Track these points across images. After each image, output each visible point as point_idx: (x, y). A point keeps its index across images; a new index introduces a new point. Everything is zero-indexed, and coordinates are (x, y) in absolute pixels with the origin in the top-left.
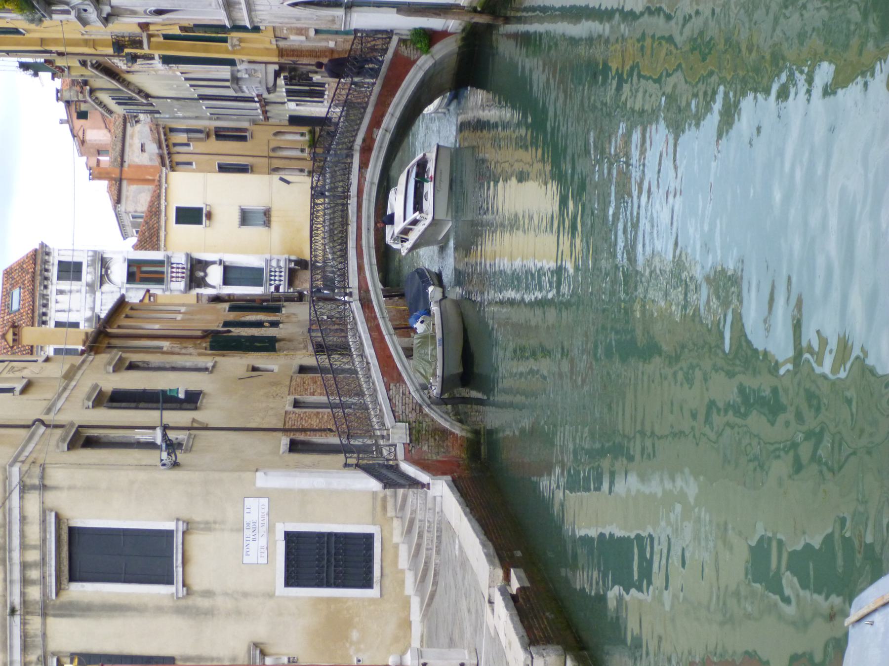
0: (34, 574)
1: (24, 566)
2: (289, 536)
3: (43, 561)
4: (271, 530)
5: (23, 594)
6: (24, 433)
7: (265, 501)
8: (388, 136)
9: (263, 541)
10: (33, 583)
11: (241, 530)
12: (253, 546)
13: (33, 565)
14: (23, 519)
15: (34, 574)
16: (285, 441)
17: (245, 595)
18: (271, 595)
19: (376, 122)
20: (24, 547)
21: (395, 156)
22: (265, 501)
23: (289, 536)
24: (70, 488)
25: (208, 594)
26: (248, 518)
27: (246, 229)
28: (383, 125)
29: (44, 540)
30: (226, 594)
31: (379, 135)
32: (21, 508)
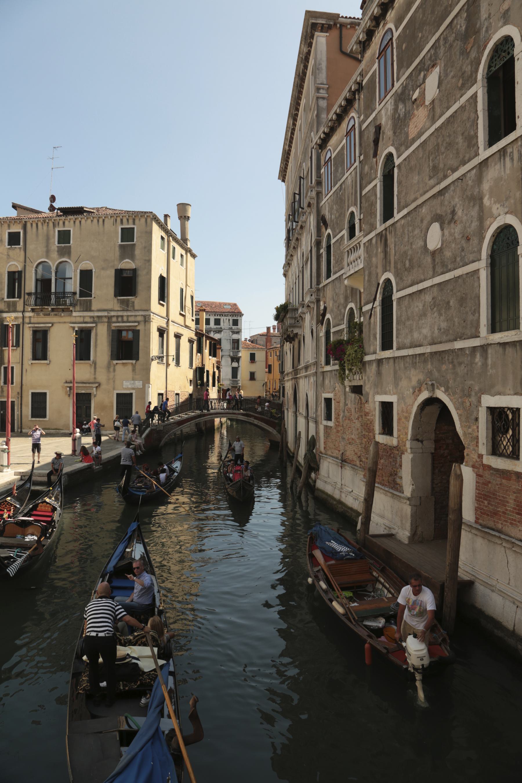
0: (120, 319)
1: (122, 316)
2: (131, 394)
3: (123, 322)
4: (133, 389)
5: (114, 316)
6: (164, 315)
7: (141, 387)
8: (252, 422)
9: (130, 386)
10: (117, 319)
11: (133, 380)
12: (128, 384)
13: (122, 319)
14: (136, 316)
15: (120, 319)
16: (163, 391)
17: (114, 382)
18: (114, 389)
19: (256, 418)
20: (128, 316)
21: (71, 471)
22: (141, 387)
23: (131, 394)
24: (145, 329)
25: (114, 370)
26: (136, 382)
27: (156, 395)
28: (255, 420)
29: (130, 322)
30: (114, 376)
31: (252, 419)
32: (139, 315)
